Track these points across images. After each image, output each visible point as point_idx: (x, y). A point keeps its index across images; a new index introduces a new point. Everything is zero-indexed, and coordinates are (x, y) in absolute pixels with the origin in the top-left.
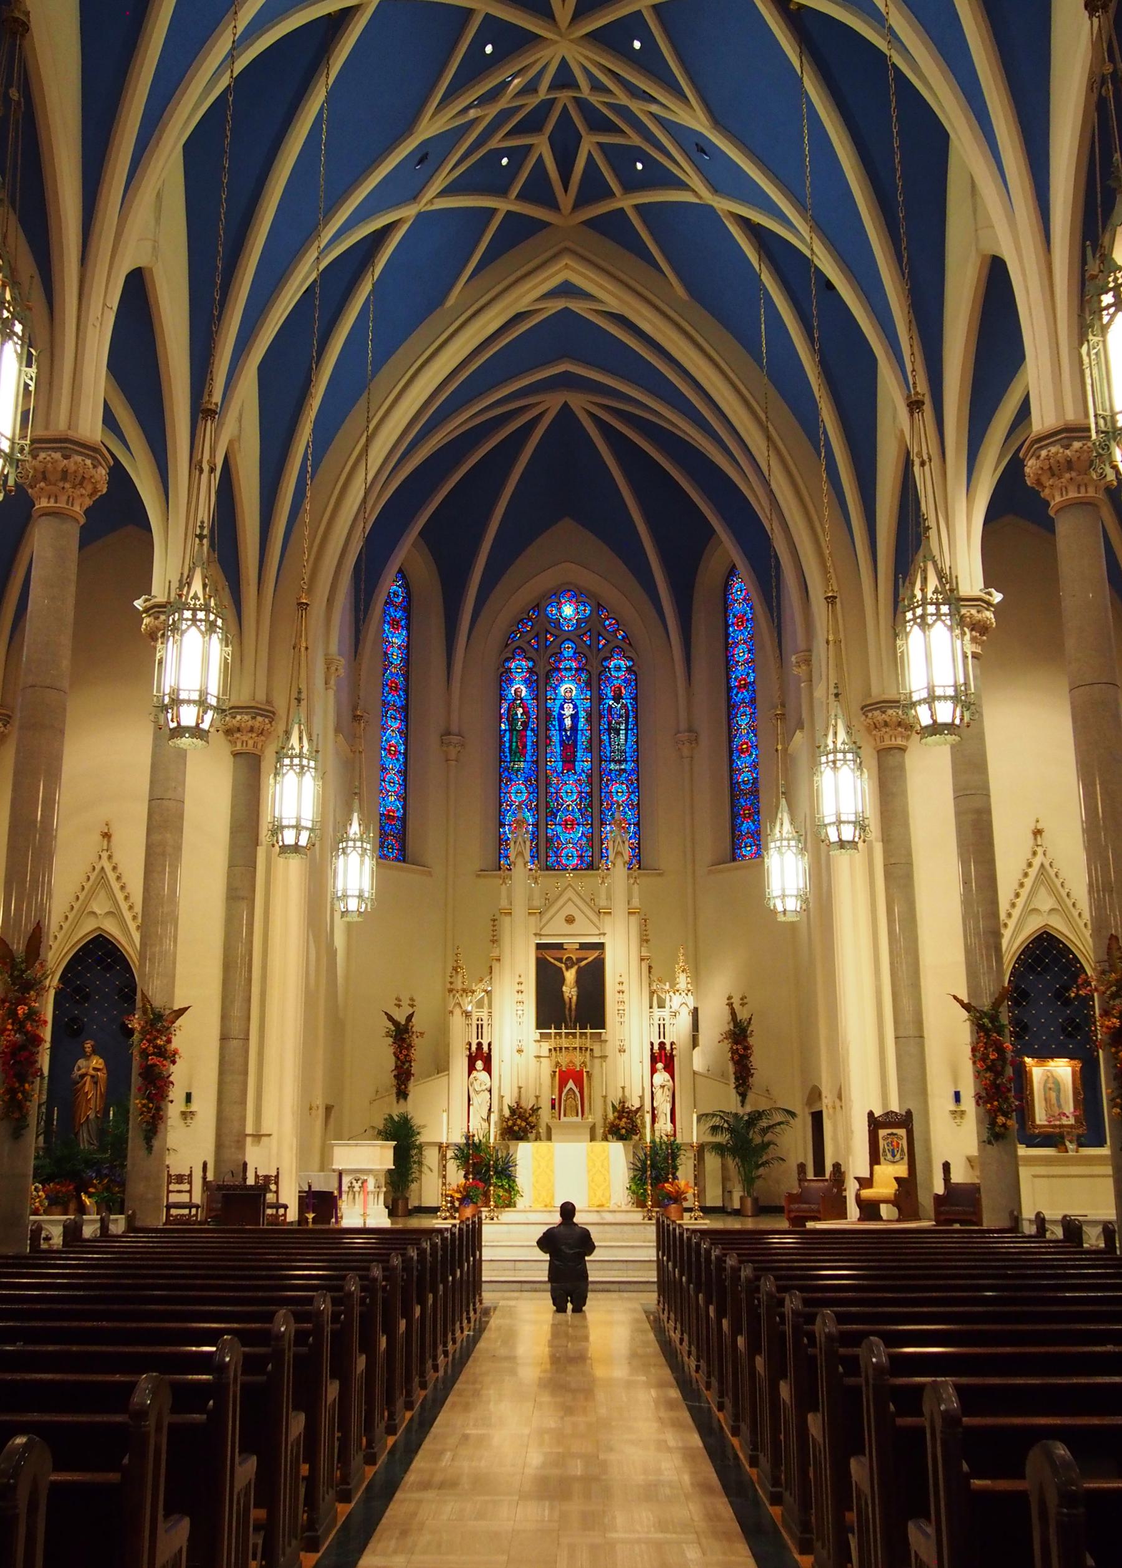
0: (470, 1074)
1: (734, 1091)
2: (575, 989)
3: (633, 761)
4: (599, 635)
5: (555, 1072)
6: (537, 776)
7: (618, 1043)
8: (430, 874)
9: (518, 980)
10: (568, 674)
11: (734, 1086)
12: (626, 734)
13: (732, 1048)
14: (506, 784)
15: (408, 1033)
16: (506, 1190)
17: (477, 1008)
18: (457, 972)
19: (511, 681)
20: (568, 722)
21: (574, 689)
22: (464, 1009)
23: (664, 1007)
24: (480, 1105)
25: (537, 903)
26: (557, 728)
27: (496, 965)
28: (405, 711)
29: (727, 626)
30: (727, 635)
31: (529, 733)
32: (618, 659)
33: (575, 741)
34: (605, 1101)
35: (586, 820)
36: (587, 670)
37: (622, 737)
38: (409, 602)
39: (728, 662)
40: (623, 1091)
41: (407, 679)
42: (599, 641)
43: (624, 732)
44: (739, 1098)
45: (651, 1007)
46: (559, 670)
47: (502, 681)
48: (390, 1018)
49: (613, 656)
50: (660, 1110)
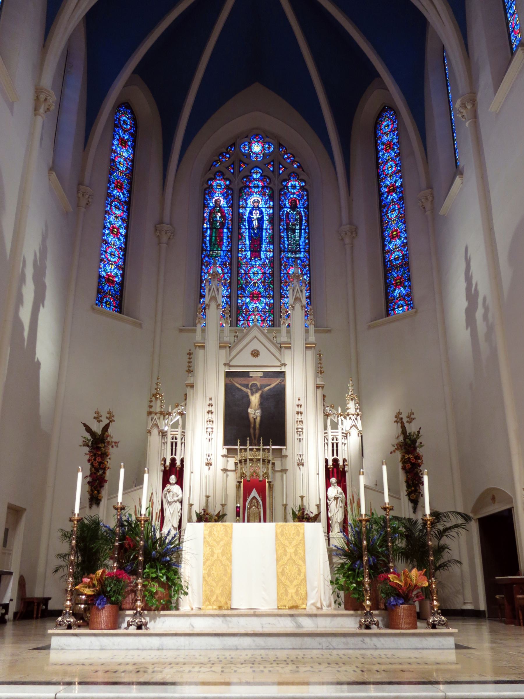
0: (164, 487)
1: (406, 498)
2: (259, 411)
3: (305, 252)
4: (280, 164)
5: (239, 482)
6: (231, 261)
7: (297, 458)
8: (140, 326)
9: (209, 402)
10: (256, 190)
11: (406, 494)
12: (300, 233)
13: (403, 458)
14: (206, 267)
15: (104, 443)
16: (162, 585)
17: (171, 428)
18: (156, 398)
19: (211, 195)
20: (255, 223)
21: (260, 200)
22: (161, 429)
23: (337, 429)
24: (172, 515)
25: (226, 339)
26: (247, 227)
27: (189, 391)
28: (128, 206)
29: (377, 152)
30: (378, 158)
31: (225, 230)
32: (294, 181)
33: (261, 237)
34: (285, 509)
35: (269, 294)
36: (271, 188)
37: (297, 234)
38: (136, 131)
39: (379, 176)
40: (302, 500)
41: (130, 183)
42: (280, 169)
43: (298, 231)
44: (411, 505)
45: (325, 428)
46: (250, 187)
47: (205, 194)
48: (88, 429)
49: (290, 179)
50: (334, 520)
